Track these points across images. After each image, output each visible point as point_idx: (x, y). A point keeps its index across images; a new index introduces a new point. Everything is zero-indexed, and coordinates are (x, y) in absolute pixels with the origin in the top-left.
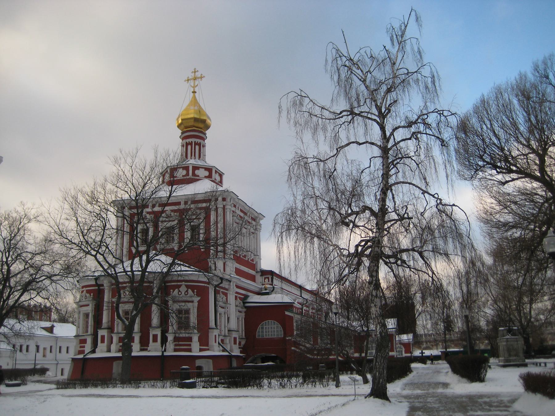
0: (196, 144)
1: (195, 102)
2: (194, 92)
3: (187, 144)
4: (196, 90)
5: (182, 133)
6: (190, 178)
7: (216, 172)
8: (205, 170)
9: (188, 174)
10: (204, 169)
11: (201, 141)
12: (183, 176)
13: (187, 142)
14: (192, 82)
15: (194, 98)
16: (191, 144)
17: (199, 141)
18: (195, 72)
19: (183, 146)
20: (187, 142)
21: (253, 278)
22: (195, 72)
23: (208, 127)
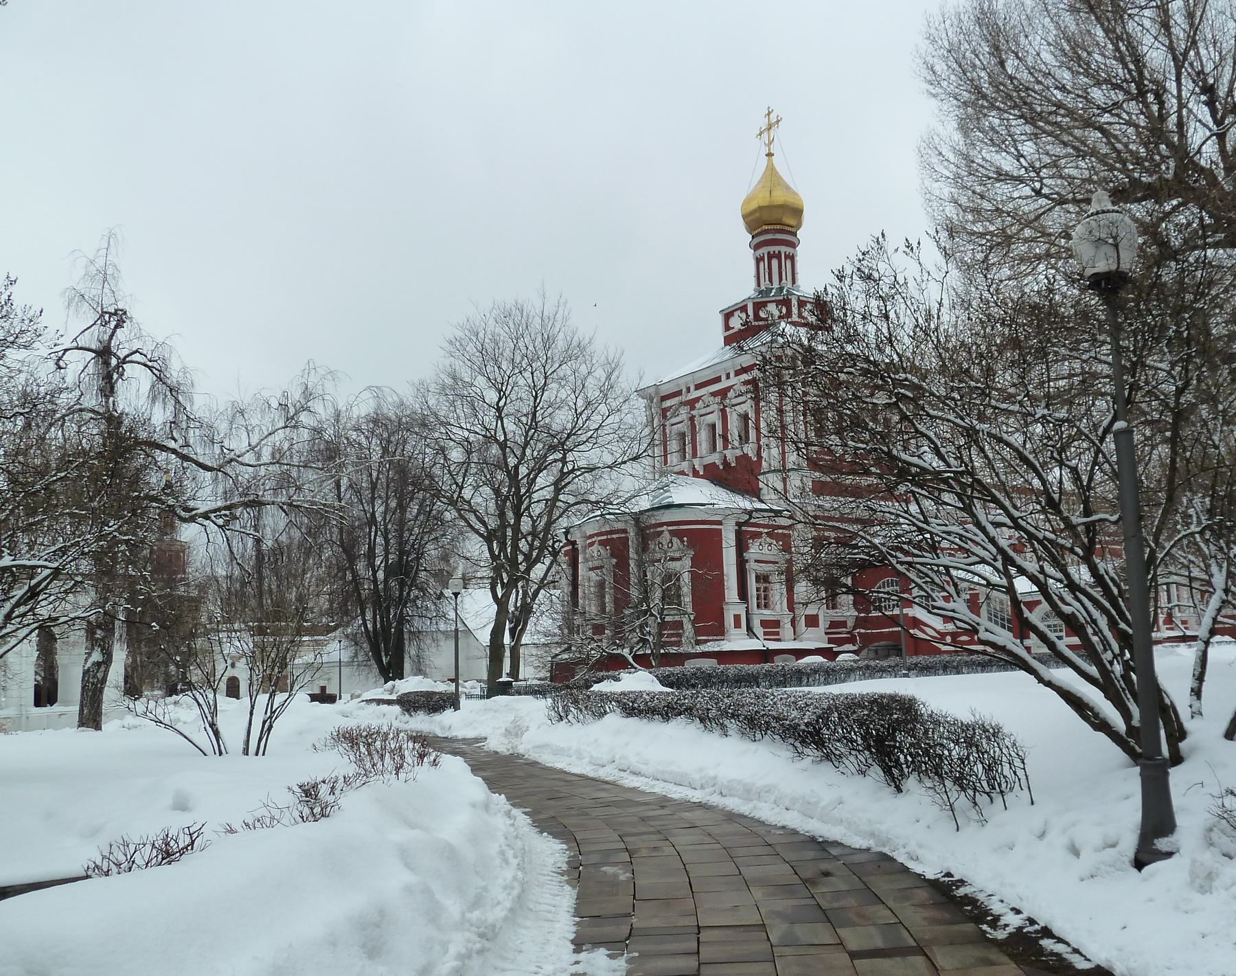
1: (771, 174)
2: (770, 155)
3: (770, 257)
5: (753, 237)
16: (778, 256)
17: (789, 250)
18: (769, 114)
19: (759, 260)
22: (769, 114)
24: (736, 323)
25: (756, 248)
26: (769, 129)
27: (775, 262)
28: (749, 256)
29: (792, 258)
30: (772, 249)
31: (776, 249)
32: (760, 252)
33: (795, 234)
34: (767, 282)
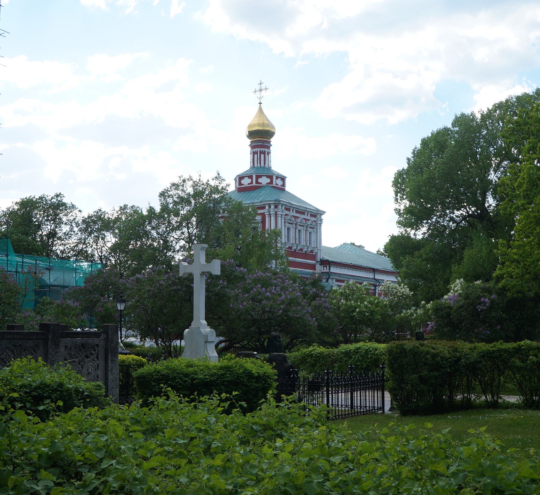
2: (260, 103)
7: (277, 178)
8: (281, 180)
9: (271, 182)
14: (258, 93)
15: (261, 110)
16: (264, 153)
18: (261, 84)
19: (254, 153)
21: (313, 267)
22: (261, 84)
24: (246, 182)
25: (252, 147)
26: (261, 90)
27: (262, 156)
29: (269, 153)
30: (262, 149)
31: (264, 149)
32: (255, 150)
33: (269, 142)
34: (259, 164)
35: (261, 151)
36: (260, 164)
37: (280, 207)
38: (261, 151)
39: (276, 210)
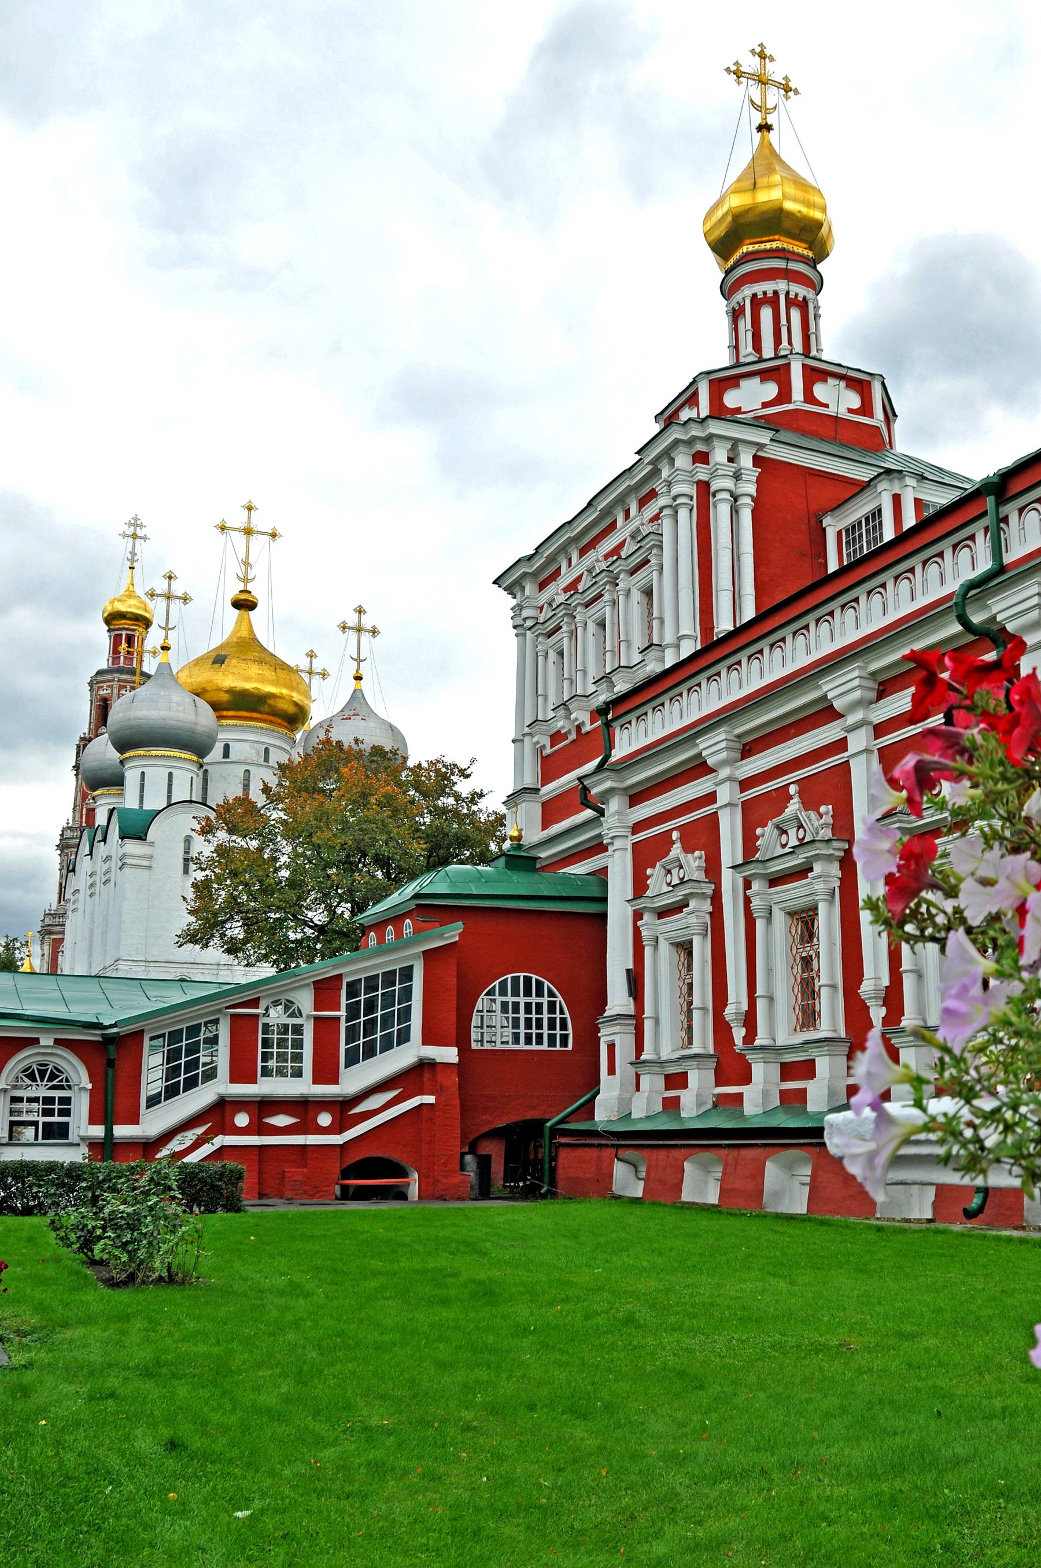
0: (790, 303)
4: (771, 119)
5: (727, 273)
6: (796, 411)
10: (843, 384)
11: (810, 294)
12: (765, 405)
13: (754, 295)
16: (773, 301)
19: (736, 315)
20: (754, 295)
23: (821, 252)
25: (727, 290)
27: (766, 314)
28: (720, 306)
29: (803, 305)
32: (738, 297)
34: (750, 349)
35: (760, 296)
36: (757, 346)
37: (720, 455)
38: (760, 296)
39: (702, 473)
